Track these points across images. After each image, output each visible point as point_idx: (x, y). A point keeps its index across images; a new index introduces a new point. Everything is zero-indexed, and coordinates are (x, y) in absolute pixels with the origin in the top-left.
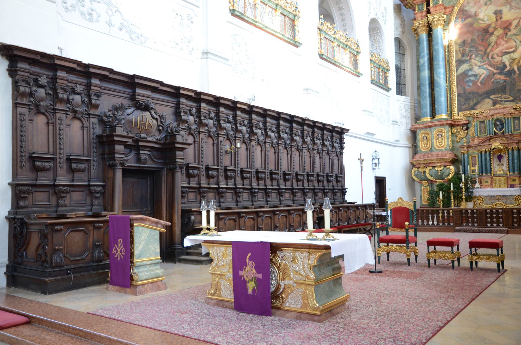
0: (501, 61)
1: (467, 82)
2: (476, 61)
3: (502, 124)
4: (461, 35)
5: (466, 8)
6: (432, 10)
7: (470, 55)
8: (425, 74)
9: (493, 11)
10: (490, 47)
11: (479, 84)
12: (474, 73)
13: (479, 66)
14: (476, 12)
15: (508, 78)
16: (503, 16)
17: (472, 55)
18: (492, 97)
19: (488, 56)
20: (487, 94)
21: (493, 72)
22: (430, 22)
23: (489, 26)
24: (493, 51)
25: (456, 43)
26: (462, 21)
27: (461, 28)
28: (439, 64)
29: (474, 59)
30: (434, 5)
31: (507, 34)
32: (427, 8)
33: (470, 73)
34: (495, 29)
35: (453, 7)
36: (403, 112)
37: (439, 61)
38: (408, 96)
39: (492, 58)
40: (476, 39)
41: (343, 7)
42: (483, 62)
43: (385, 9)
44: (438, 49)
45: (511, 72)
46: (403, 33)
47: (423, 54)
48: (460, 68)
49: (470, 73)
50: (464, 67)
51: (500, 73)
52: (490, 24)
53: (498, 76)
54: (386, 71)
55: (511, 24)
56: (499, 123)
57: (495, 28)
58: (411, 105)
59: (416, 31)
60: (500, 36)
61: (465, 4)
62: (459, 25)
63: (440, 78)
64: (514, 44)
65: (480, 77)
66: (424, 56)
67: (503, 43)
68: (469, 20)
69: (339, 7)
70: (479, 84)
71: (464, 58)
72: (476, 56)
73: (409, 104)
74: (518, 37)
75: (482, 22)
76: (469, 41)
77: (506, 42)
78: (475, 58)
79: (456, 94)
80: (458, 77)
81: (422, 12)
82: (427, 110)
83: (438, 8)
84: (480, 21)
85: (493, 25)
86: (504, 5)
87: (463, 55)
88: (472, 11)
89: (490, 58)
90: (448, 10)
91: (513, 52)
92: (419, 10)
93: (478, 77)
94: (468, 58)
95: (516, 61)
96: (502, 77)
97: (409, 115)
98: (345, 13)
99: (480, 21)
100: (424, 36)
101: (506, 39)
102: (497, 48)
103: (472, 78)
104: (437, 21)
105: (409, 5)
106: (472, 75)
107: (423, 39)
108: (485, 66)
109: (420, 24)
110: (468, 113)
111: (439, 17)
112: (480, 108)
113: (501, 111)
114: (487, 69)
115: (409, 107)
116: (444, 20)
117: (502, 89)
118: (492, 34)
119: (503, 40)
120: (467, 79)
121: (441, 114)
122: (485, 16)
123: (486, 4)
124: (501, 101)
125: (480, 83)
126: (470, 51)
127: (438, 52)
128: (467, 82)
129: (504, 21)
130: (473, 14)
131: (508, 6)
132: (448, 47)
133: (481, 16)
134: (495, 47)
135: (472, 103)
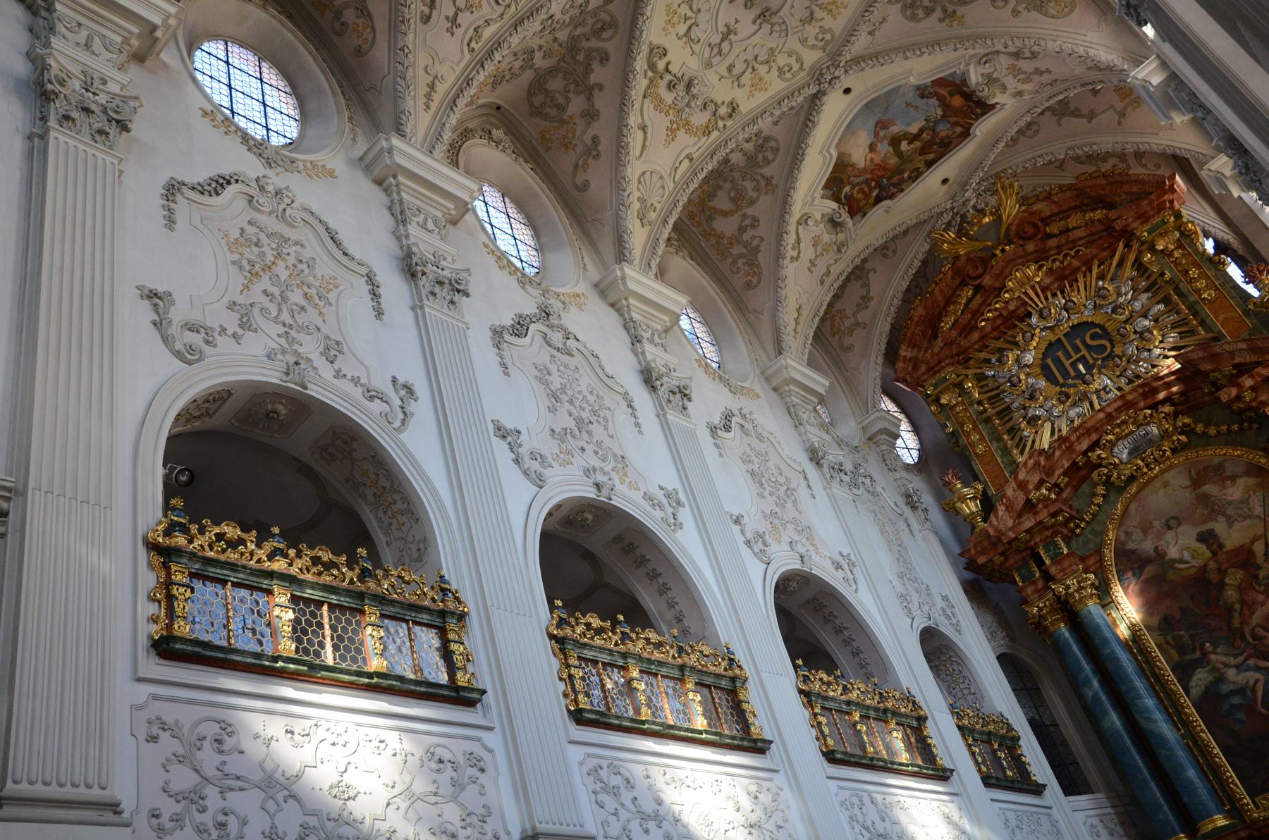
4: (1149, 606)
5: (1131, 546)
6: (1053, 571)
7: (1197, 645)
8: (1113, 723)
9: (1195, 537)
10: (1236, 615)
11: (1263, 711)
12: (1232, 687)
13: (1236, 666)
14: (1156, 548)
16: (1222, 540)
17: (1202, 645)
22: (1063, 598)
23: (1204, 568)
24: (1248, 623)
25: (1148, 628)
26: (1134, 575)
27: (1141, 593)
28: (1135, 689)
29: (1215, 653)
30: (1052, 559)
31: (1256, 577)
32: (1041, 571)
34: (1223, 572)
35: (1099, 552)
37: (1131, 681)
38: (1099, 792)
39: (1255, 637)
41: (845, 625)
42: (1240, 654)
43: (945, 598)
44: (1113, 652)
46: (1011, 638)
47: (1083, 676)
48: (1192, 684)
49: (1225, 688)
50: (1201, 678)
52: (1205, 566)
54: (1010, 742)
55: (1251, 553)
57: (1219, 570)
58: (1117, 814)
60: (1244, 585)
61: (1122, 538)
62: (1133, 587)
63: (1154, 721)
65: (1254, 690)
68: (1149, 570)
69: (835, 628)
70: (1263, 711)
72: (1215, 645)
73: (1110, 810)
75: (1183, 566)
76: (1178, 615)
78: (1215, 648)
79: (1217, 751)
81: (1034, 583)
82: (1167, 814)
83: (1066, 564)
84: (1177, 565)
85: (1212, 565)
86: (1211, 520)
87: (1182, 652)
88: (1148, 546)
89: (1250, 640)
90: (1091, 562)
92: (1024, 579)
93: (1249, 693)
98: (853, 637)
99: (1177, 565)
100: (1064, 631)
101: (1262, 588)
102: (1253, 613)
103: (1236, 700)
104: (1077, 591)
105: (997, 574)
106: (1232, 693)
107: (1066, 640)
108: (1251, 662)
109: (1040, 609)
111: (1079, 582)
114: (1257, 669)
115: (1116, 820)
116: (1093, 584)
118: (1222, 585)
119: (1257, 591)
120: (1226, 707)
121: (1210, 816)
122: (1181, 551)
123: (1169, 528)
125: (1263, 707)
127: (1118, 659)
129: (1232, 551)
130: (1152, 553)
131: (1222, 519)
132: (1134, 641)
133: (1173, 553)
134: (1246, 610)
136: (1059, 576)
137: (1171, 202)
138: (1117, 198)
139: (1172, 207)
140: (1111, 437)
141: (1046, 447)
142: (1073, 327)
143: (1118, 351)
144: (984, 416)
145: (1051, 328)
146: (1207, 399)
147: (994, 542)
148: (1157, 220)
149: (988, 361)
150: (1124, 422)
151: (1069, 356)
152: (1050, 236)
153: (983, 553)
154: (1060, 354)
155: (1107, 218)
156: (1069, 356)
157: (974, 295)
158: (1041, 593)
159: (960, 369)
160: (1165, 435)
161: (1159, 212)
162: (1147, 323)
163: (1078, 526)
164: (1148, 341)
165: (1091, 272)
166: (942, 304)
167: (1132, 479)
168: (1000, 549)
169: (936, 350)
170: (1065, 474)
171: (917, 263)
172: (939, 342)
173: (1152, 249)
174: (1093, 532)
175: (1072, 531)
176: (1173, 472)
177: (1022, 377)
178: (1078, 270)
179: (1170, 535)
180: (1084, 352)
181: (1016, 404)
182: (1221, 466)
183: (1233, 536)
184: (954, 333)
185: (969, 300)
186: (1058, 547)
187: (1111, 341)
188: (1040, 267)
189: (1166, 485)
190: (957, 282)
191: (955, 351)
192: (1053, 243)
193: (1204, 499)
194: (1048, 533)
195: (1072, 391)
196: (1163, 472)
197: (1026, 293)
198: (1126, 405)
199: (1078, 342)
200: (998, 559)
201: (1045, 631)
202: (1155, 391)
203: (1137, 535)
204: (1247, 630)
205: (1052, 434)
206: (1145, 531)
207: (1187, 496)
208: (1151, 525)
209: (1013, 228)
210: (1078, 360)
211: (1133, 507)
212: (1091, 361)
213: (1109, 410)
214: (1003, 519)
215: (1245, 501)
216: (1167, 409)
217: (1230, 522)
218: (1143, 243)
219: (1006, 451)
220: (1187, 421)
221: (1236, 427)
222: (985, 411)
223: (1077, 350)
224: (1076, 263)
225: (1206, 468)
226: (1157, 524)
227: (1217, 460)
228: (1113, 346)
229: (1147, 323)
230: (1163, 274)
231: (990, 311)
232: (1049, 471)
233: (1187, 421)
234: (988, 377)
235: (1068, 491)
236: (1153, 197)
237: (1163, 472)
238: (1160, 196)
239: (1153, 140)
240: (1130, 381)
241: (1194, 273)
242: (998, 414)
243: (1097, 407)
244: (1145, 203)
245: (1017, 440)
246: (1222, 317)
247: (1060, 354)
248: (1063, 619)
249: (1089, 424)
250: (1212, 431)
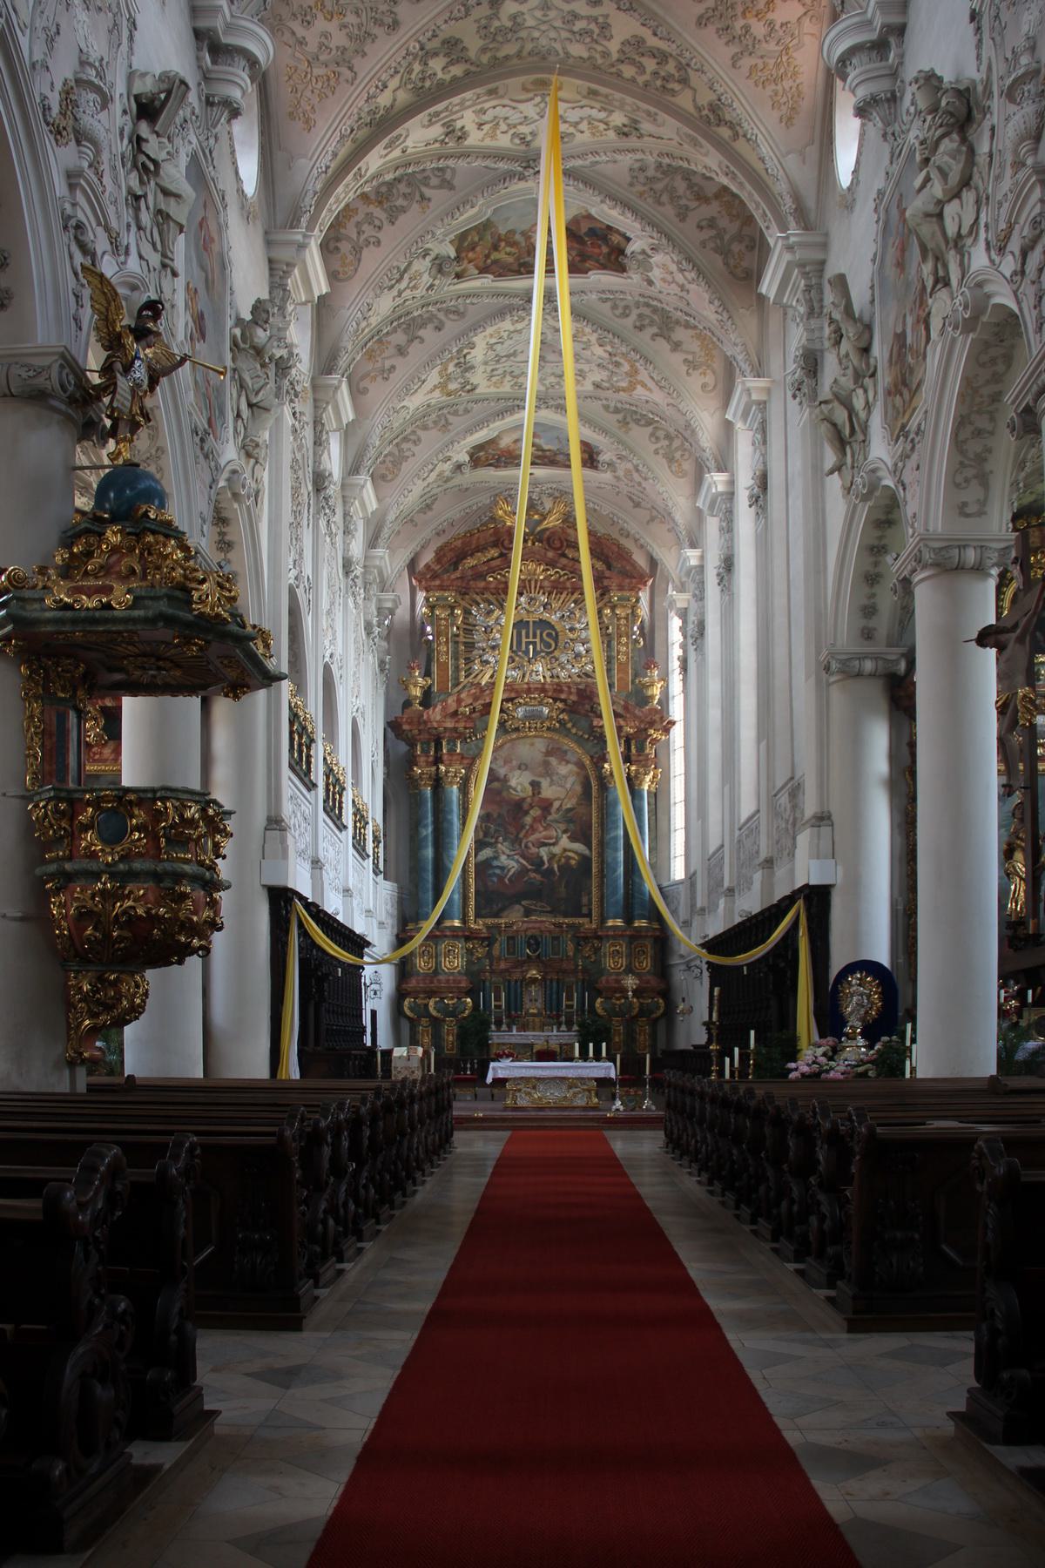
0: (538, 853)
1: (490, 876)
2: (503, 847)
3: (538, 944)
9: (530, 780)
10: (524, 831)
12: (500, 864)
13: (508, 856)
14: (505, 776)
15: (545, 880)
18: (523, 903)
19: (521, 843)
20: (516, 899)
21: (526, 867)
23: (524, 799)
28: (452, 843)
30: (448, 751)
32: (436, 752)
33: (495, 863)
34: (531, 807)
36: (389, 907)
39: (526, 846)
40: (505, 814)
45: (550, 871)
49: (495, 863)
50: (487, 853)
51: (534, 871)
53: (533, 875)
55: (551, 805)
56: (534, 942)
59: (412, 783)
64: (555, 834)
65: (509, 871)
66: (426, 826)
67: (541, 829)
71: (487, 839)
72: (504, 840)
74: (560, 825)
76: (495, 816)
77: (546, 829)
83: (455, 758)
85: (529, 800)
87: (486, 835)
90: (465, 762)
91: (554, 844)
92: (423, 750)
94: (493, 840)
95: (557, 858)
96: (538, 877)
97: (395, 913)
103: (498, 871)
108: (516, 857)
109: (422, 773)
110: (489, 921)
112: (507, 917)
113: (537, 925)
114: (518, 862)
117: (535, 893)
118: (527, 813)
120: (491, 872)
122: (518, 784)
123: (519, 768)
124: (535, 910)
126: (496, 831)
128: (490, 876)
130: (502, 776)
131: (548, 779)
133: (513, 783)
135: (495, 908)
136: (447, 762)
137: (640, 589)
138: (615, 564)
139: (637, 592)
140: (521, 701)
141: (483, 683)
142: (541, 620)
143: (556, 654)
144: (457, 639)
145: (528, 611)
146: (583, 712)
147: (419, 721)
148: (627, 594)
149: (478, 604)
150: (535, 698)
151: (527, 637)
152: (564, 555)
153: (409, 724)
154: (524, 632)
155: (603, 572)
156: (527, 637)
157: (498, 558)
158: (428, 764)
159: (459, 599)
160: (550, 718)
161: (632, 590)
162: (582, 649)
163: (470, 737)
164: (577, 661)
165: (572, 594)
166: (473, 547)
167: (517, 729)
168: (421, 727)
169: (453, 577)
170: (483, 705)
171: (475, 508)
172: (458, 574)
173: (613, 608)
174: (477, 746)
175: (466, 739)
176: (540, 740)
177: (494, 631)
178: (566, 589)
179: (517, 773)
180: (538, 640)
181: (480, 645)
182: (566, 752)
183: (548, 791)
184: (470, 573)
185: (493, 559)
186: (455, 745)
187: (556, 645)
188: (548, 570)
189: (532, 744)
190: (492, 539)
191: (464, 585)
192: (564, 561)
193: (546, 764)
194: (455, 735)
195: (517, 659)
196: (535, 736)
197: (530, 581)
198: (542, 689)
199: (538, 632)
200: (416, 732)
201: (417, 787)
202: (561, 691)
204: (524, 841)
205: (492, 677)
206: (506, 762)
207: (539, 757)
208: (511, 761)
209: (548, 533)
210: (531, 643)
211: (508, 745)
212: (538, 648)
213: (531, 686)
214: (435, 714)
215: (565, 777)
216: (560, 705)
217: (552, 782)
218: (610, 602)
219: (457, 669)
220: (566, 718)
221: (586, 736)
222: (458, 636)
223: (535, 637)
224: (568, 584)
225: (558, 749)
226: (514, 763)
227: (566, 748)
228: (555, 649)
229: (582, 649)
230: (608, 628)
231: (500, 574)
232: (476, 699)
233: (566, 718)
234: (471, 614)
235: (478, 714)
236: (634, 581)
237: (535, 736)
238: (638, 583)
239: (654, 546)
240: (552, 677)
241: (624, 640)
242: (465, 643)
243: (526, 680)
244: (627, 581)
245: (467, 667)
246: (620, 675)
247: (524, 632)
248: (431, 786)
249: (516, 687)
250: (574, 731)
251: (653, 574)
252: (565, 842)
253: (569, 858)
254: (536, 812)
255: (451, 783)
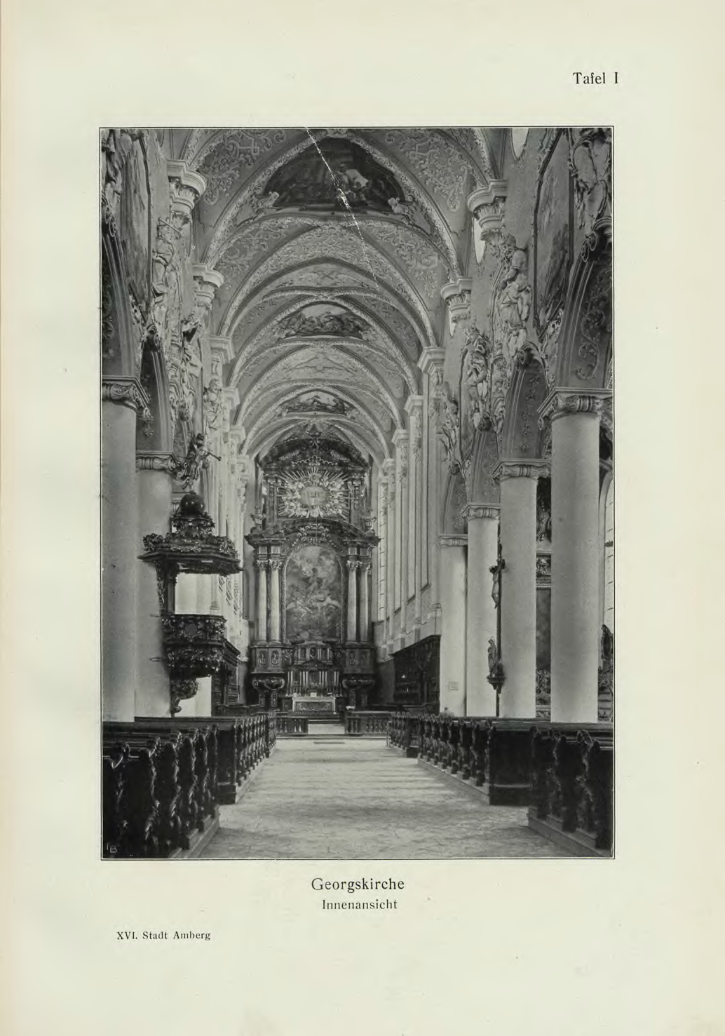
18: (309, 630)
50: (292, 605)
80: (287, 611)
87: (292, 595)
118: (310, 584)
133: (304, 569)
183: (321, 574)
203: (298, 558)
251: (372, 465)
252: (329, 600)
253: (331, 608)
254: (315, 584)
255: (275, 569)
